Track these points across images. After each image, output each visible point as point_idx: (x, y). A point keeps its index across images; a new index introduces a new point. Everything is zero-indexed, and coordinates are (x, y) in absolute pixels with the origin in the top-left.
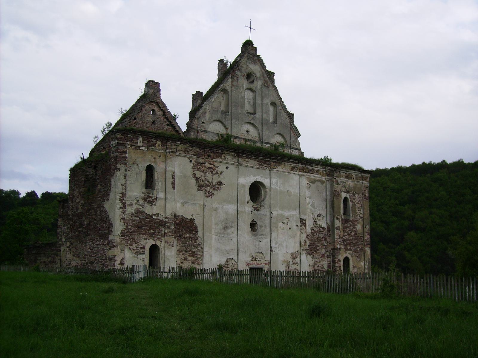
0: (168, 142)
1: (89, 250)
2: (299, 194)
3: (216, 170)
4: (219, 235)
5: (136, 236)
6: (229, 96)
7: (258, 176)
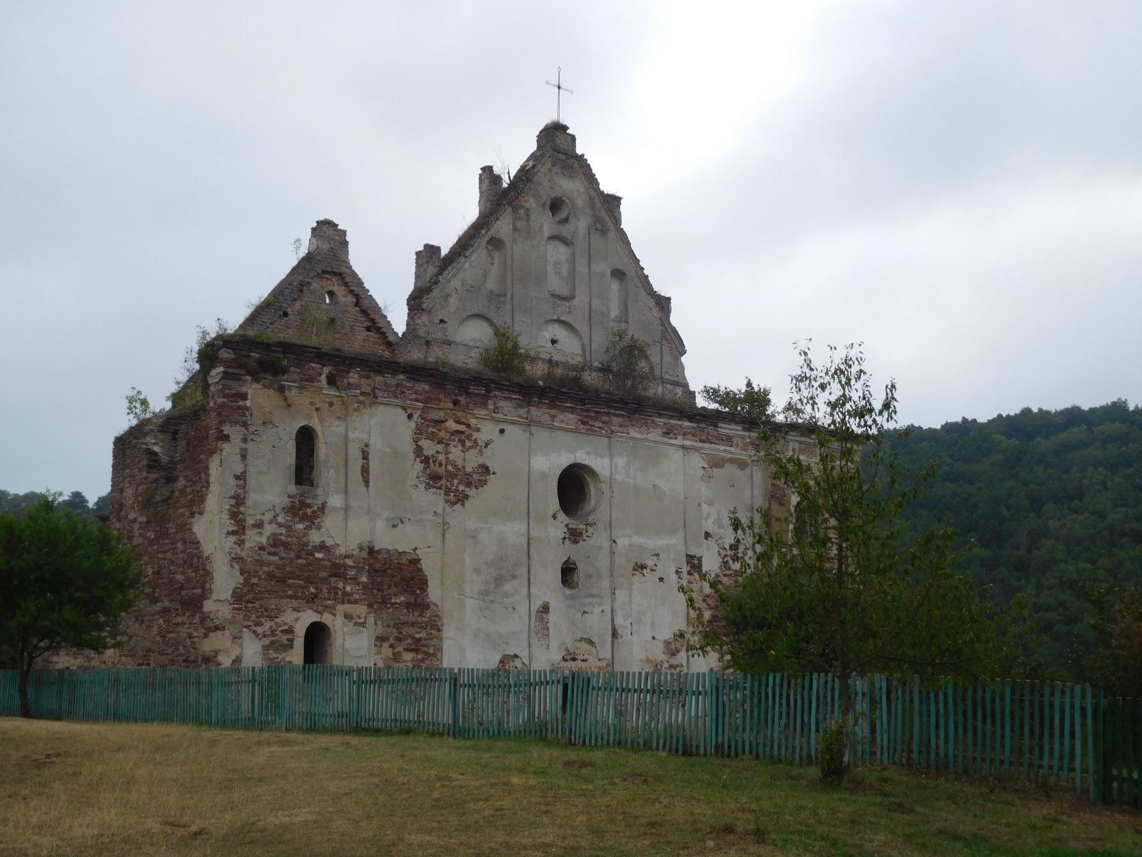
0: (352, 370)
1: (158, 638)
2: (685, 494)
3: (473, 439)
4: (482, 597)
5: (272, 603)
6: (505, 255)
7: (579, 451)
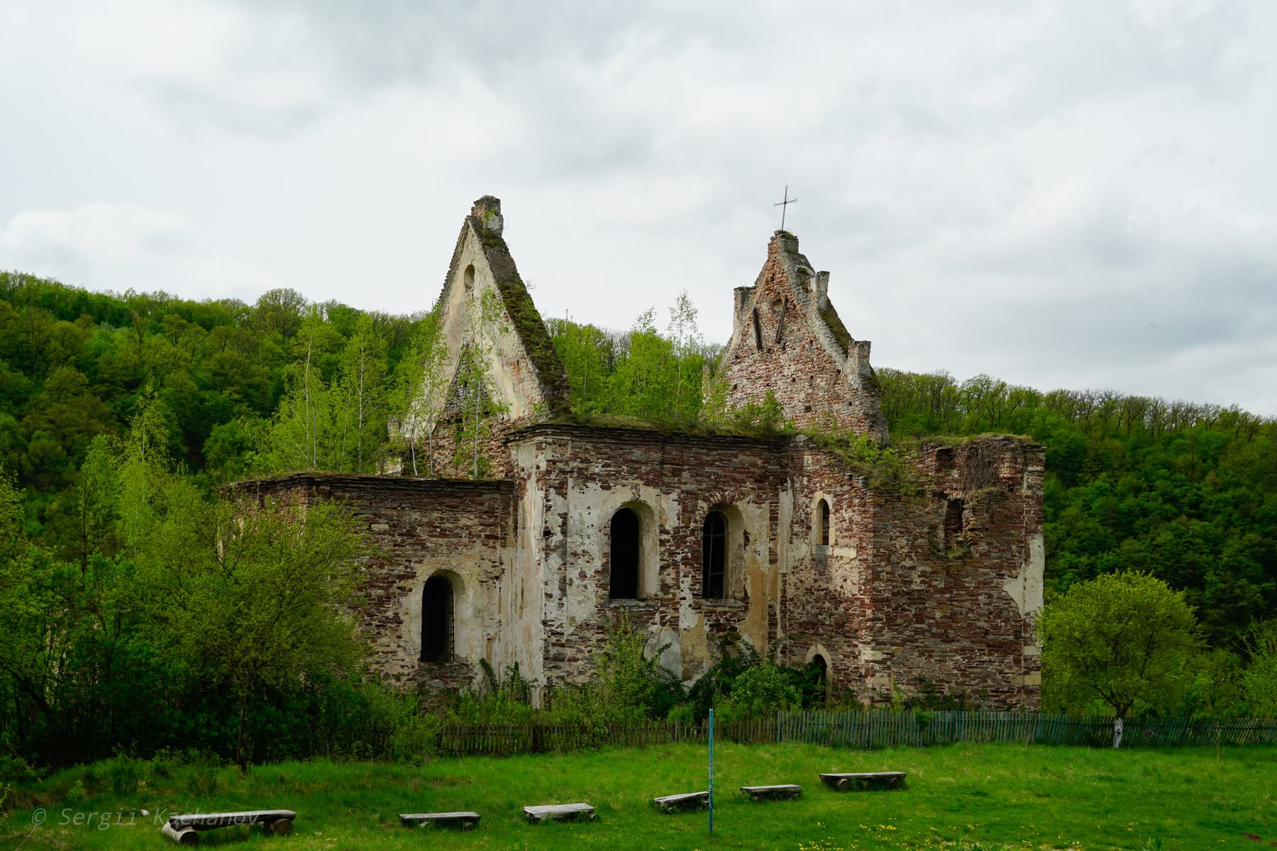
1: (955, 671)
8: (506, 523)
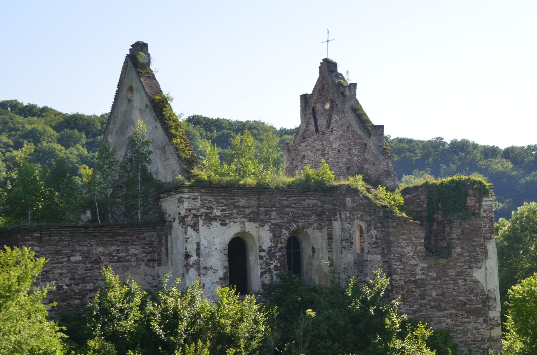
8: (161, 250)
